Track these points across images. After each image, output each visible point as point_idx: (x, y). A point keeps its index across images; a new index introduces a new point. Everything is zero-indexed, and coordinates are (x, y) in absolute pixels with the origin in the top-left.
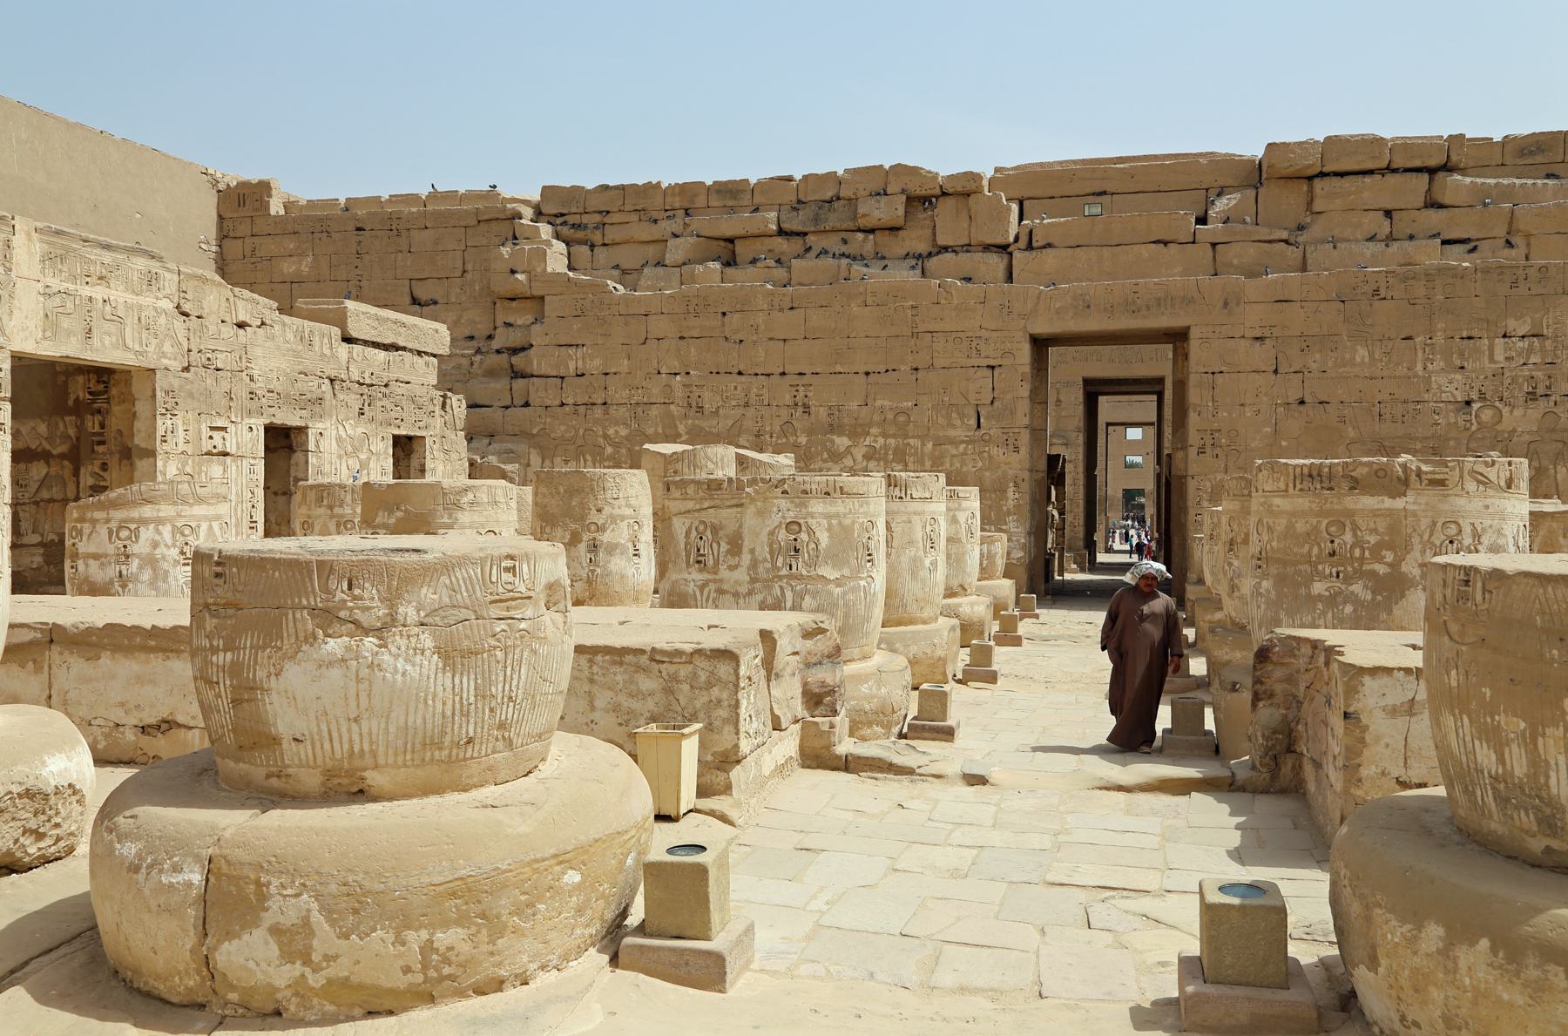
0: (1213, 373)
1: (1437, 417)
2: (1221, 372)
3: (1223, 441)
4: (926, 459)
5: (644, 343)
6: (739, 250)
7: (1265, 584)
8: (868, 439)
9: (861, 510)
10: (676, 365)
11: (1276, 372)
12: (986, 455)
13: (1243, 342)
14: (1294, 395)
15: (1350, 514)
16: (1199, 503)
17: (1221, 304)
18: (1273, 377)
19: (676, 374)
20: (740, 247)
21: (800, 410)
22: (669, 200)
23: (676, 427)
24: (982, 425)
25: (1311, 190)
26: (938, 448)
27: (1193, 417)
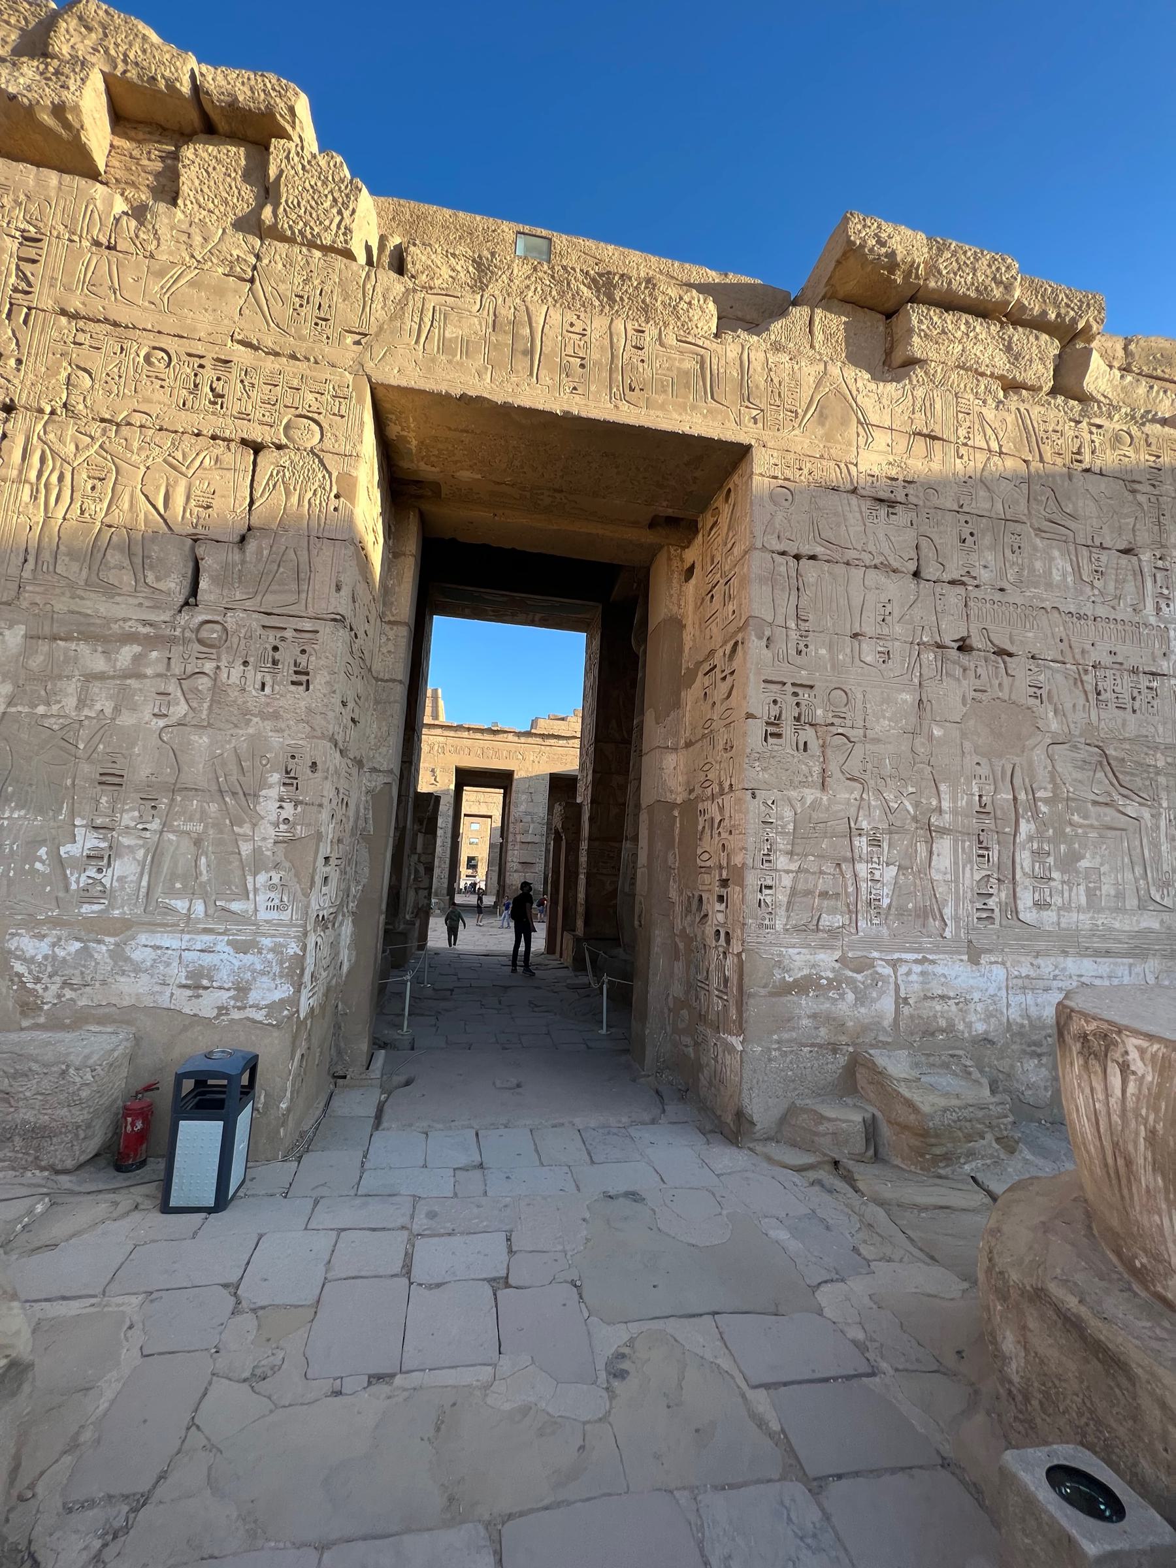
0: (797, 557)
2: (813, 557)
3: (819, 712)
11: (916, 574)
26: (44, 647)
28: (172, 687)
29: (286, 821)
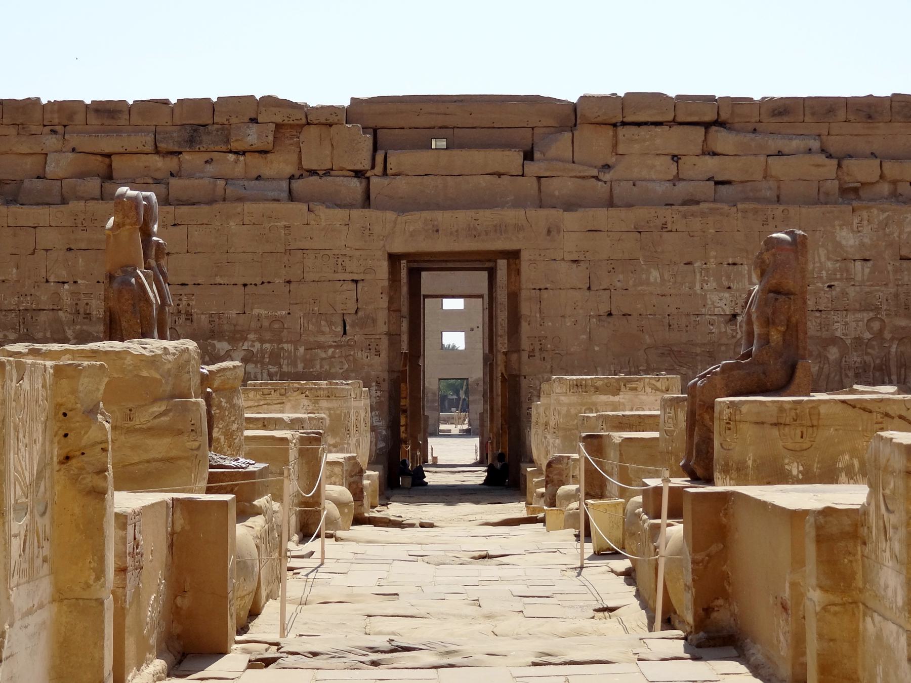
0: (540, 289)
1: (711, 327)
2: (546, 289)
3: (549, 346)
4: (299, 362)
5: (33, 253)
6: (115, 165)
7: (557, 441)
8: (246, 344)
9: (345, 405)
10: (64, 274)
11: (589, 288)
12: (351, 358)
13: (563, 264)
14: (604, 309)
15: (595, 404)
16: (530, 399)
17: (545, 231)
18: (587, 293)
19: (64, 283)
20: (116, 162)
21: (183, 317)
22: (48, 116)
23: (64, 332)
24: (347, 332)
25: (615, 136)
26: (309, 351)
27: (525, 327)
28: (343, 360)
29: (378, 396)
